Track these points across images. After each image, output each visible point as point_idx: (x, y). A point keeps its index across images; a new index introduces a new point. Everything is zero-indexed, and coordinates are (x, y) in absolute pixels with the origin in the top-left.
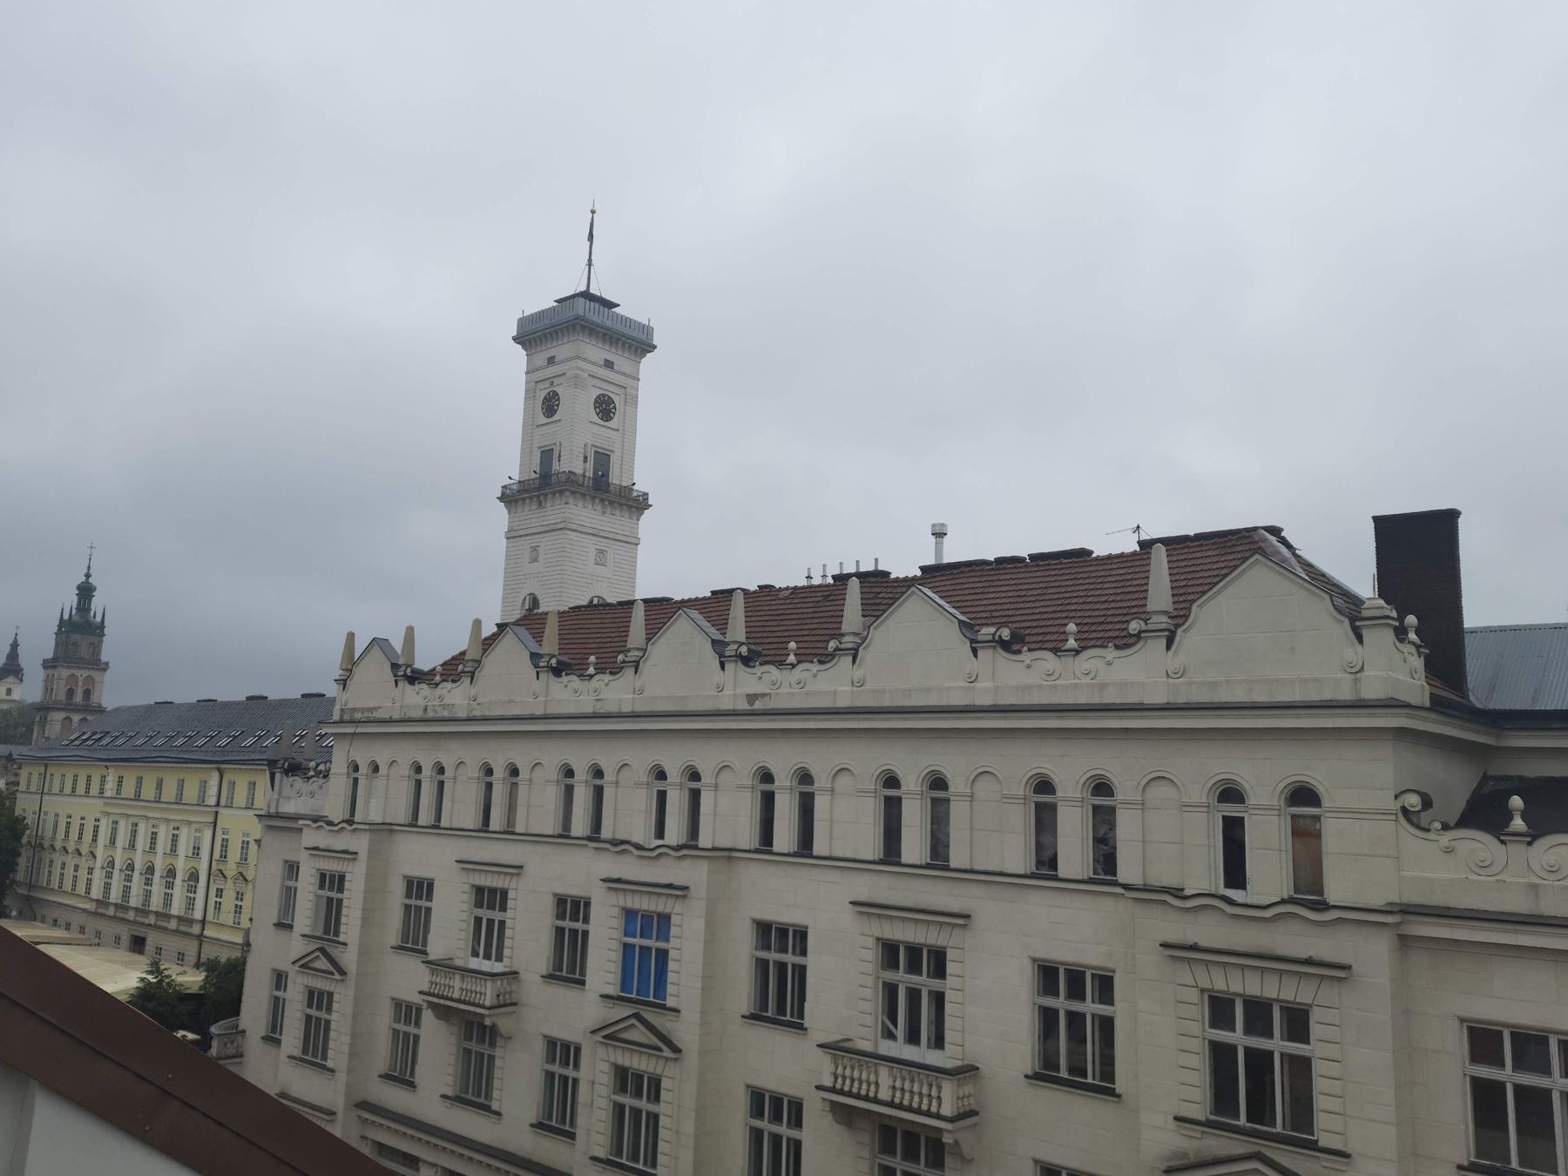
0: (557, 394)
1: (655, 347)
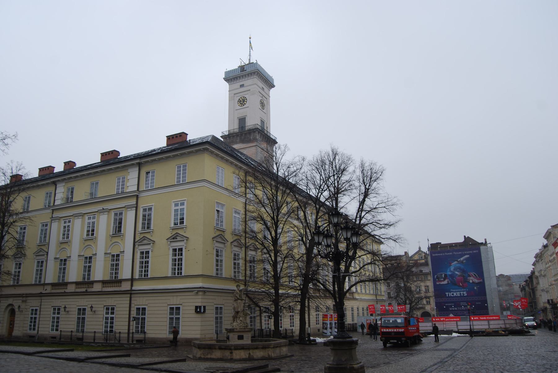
0: (245, 98)
1: (274, 86)
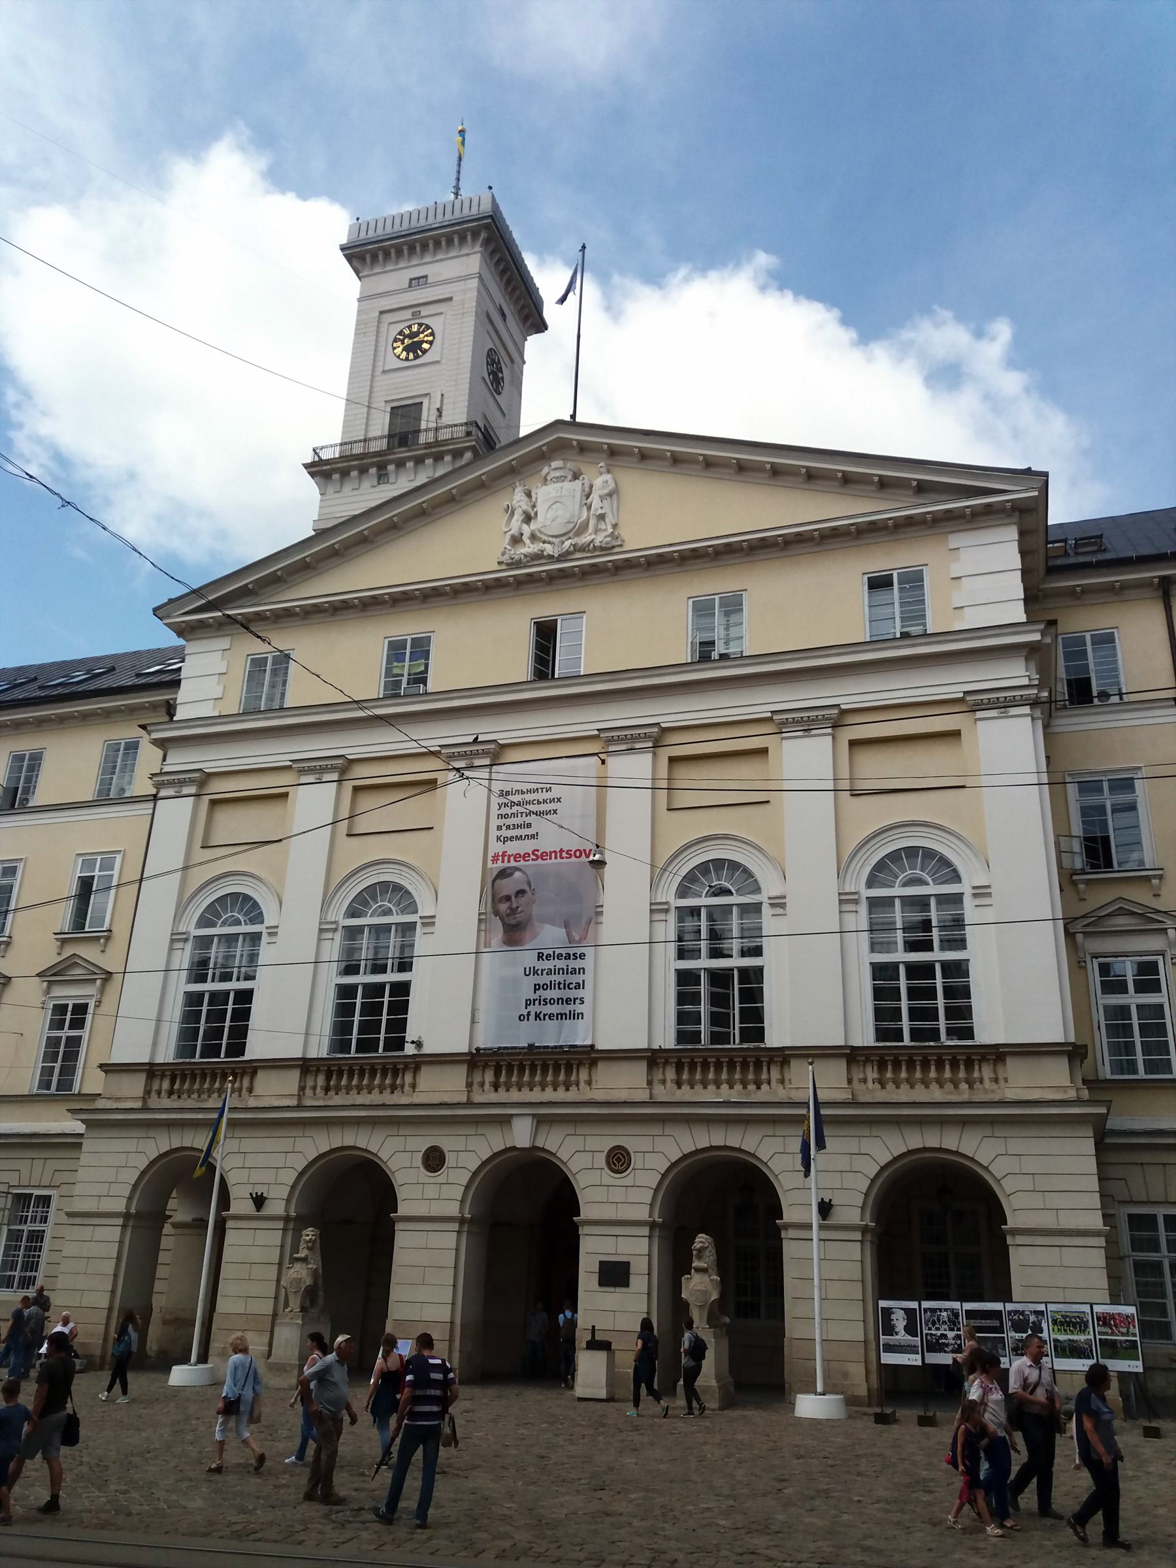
0: (428, 327)
